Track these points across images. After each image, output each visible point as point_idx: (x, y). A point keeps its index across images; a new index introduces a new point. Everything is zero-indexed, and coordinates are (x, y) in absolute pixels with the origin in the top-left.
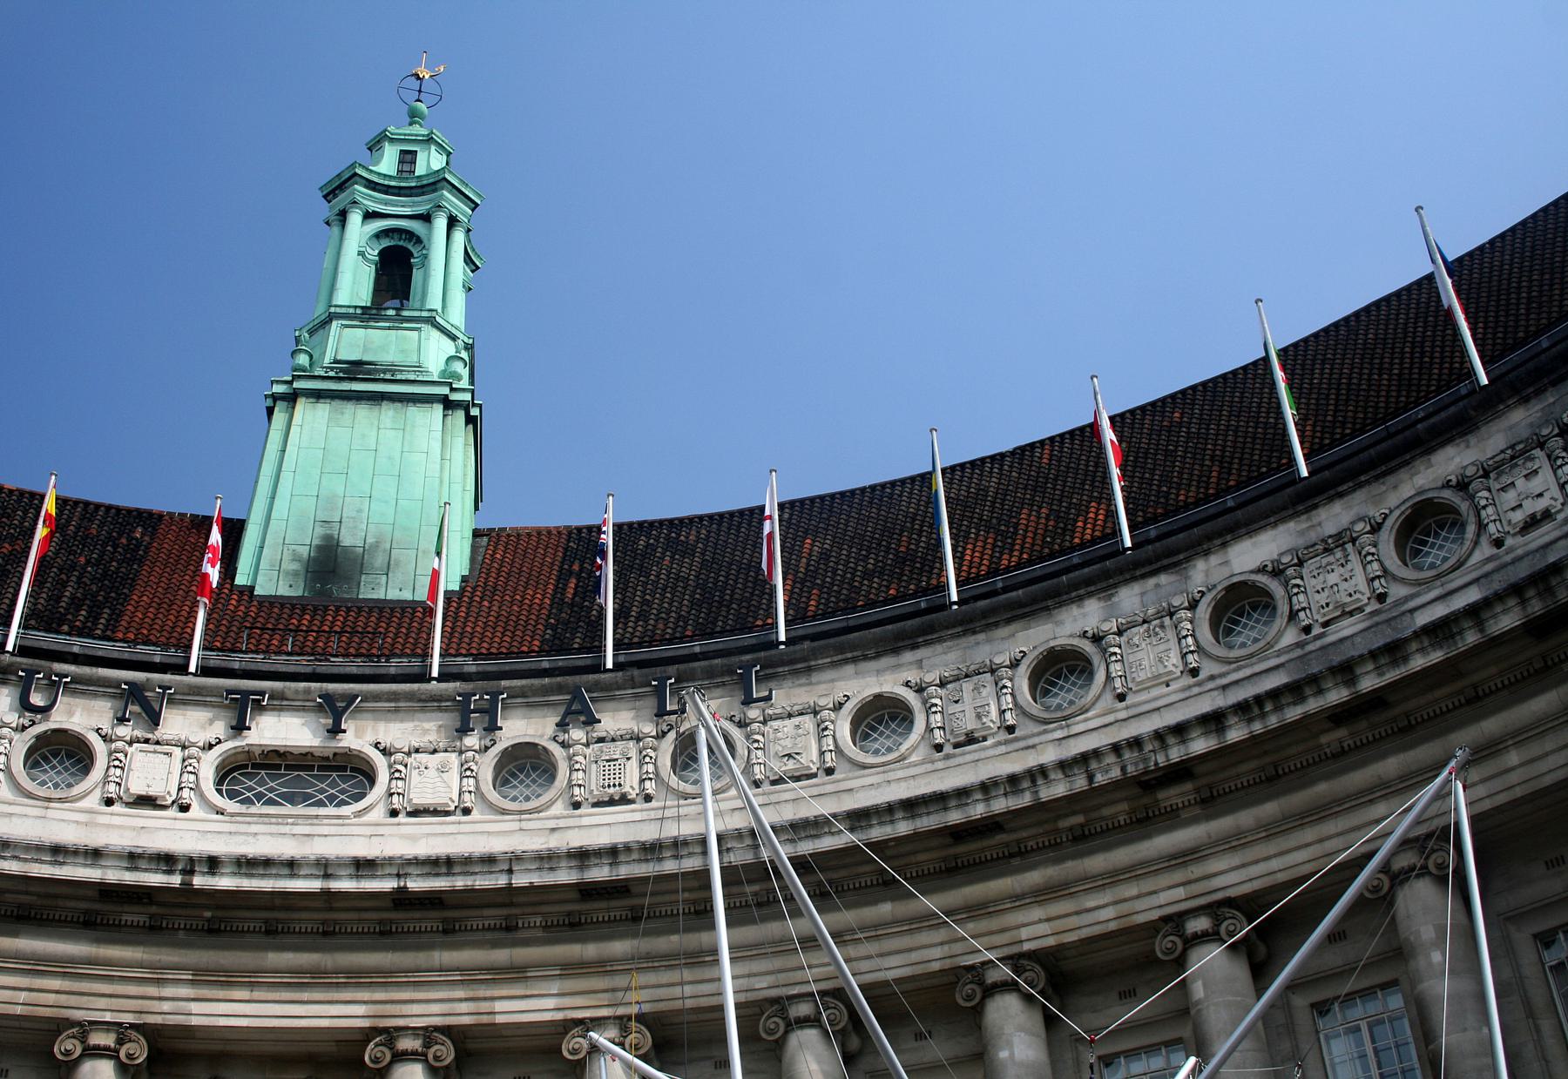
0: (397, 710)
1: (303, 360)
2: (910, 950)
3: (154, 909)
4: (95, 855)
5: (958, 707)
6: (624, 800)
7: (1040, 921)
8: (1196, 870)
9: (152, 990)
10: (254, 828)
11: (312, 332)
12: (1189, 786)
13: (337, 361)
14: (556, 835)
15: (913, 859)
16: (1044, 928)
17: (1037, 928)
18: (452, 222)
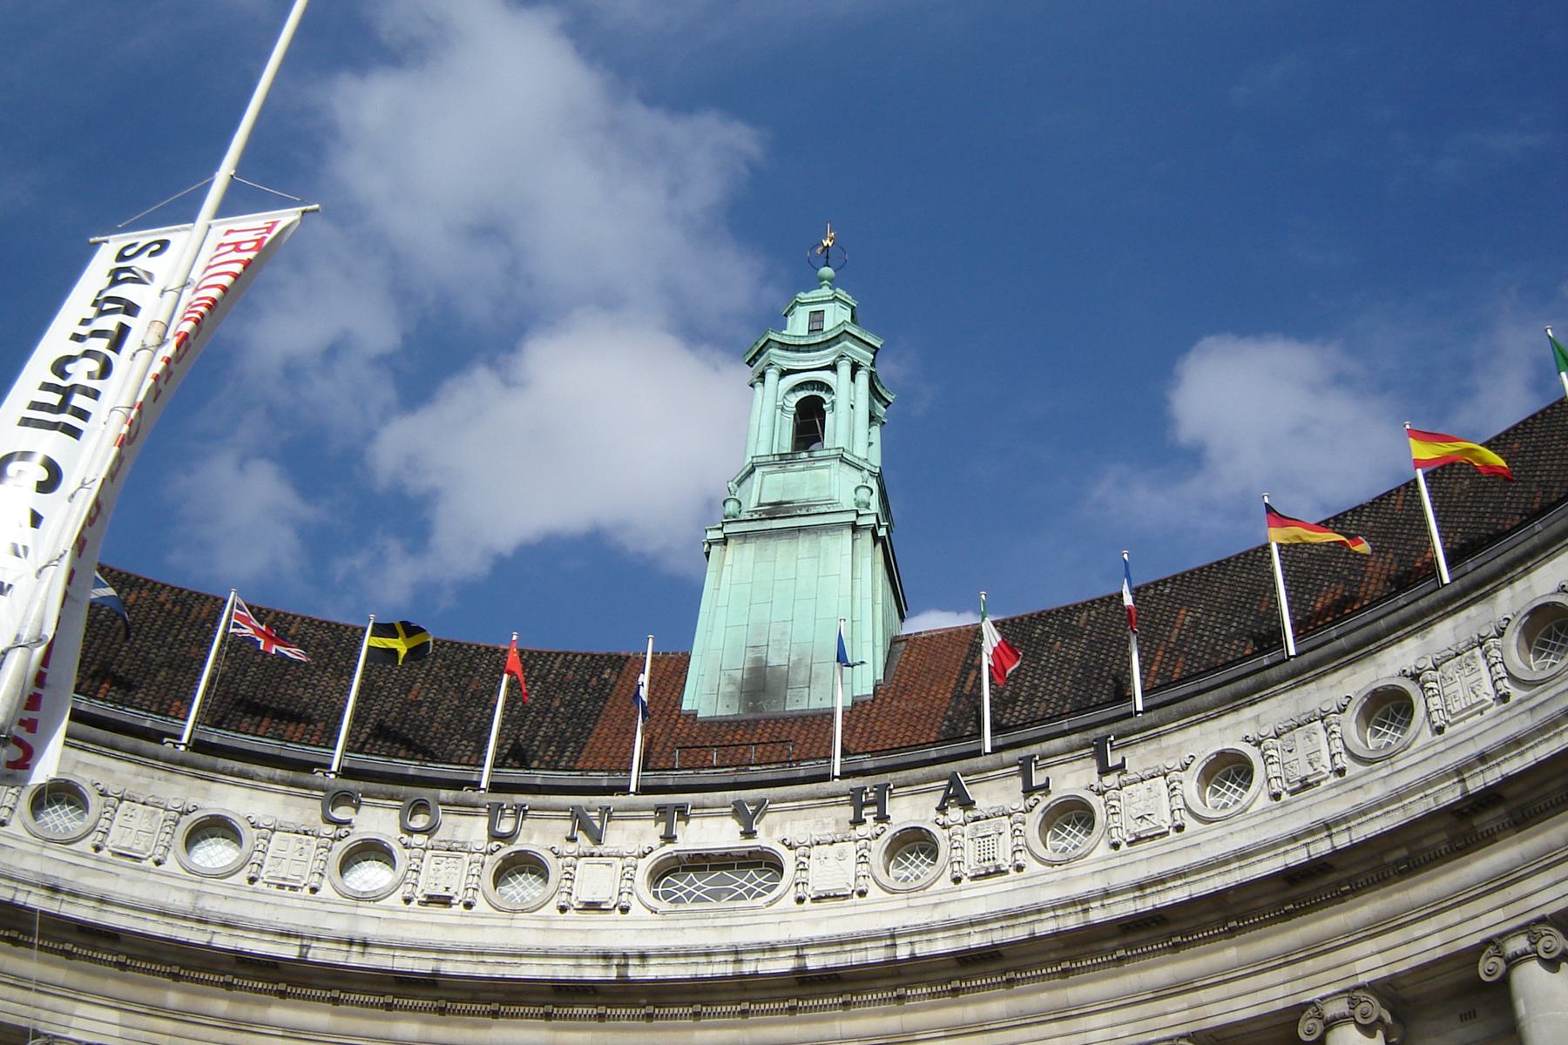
0: (801, 808)
1: (731, 507)
5: (1291, 756)
6: (999, 872)
7: (1373, 954)
10: (681, 924)
11: (739, 483)
12: (1501, 810)
13: (760, 505)
14: (940, 909)
16: (1377, 960)
17: (1372, 961)
18: (855, 367)
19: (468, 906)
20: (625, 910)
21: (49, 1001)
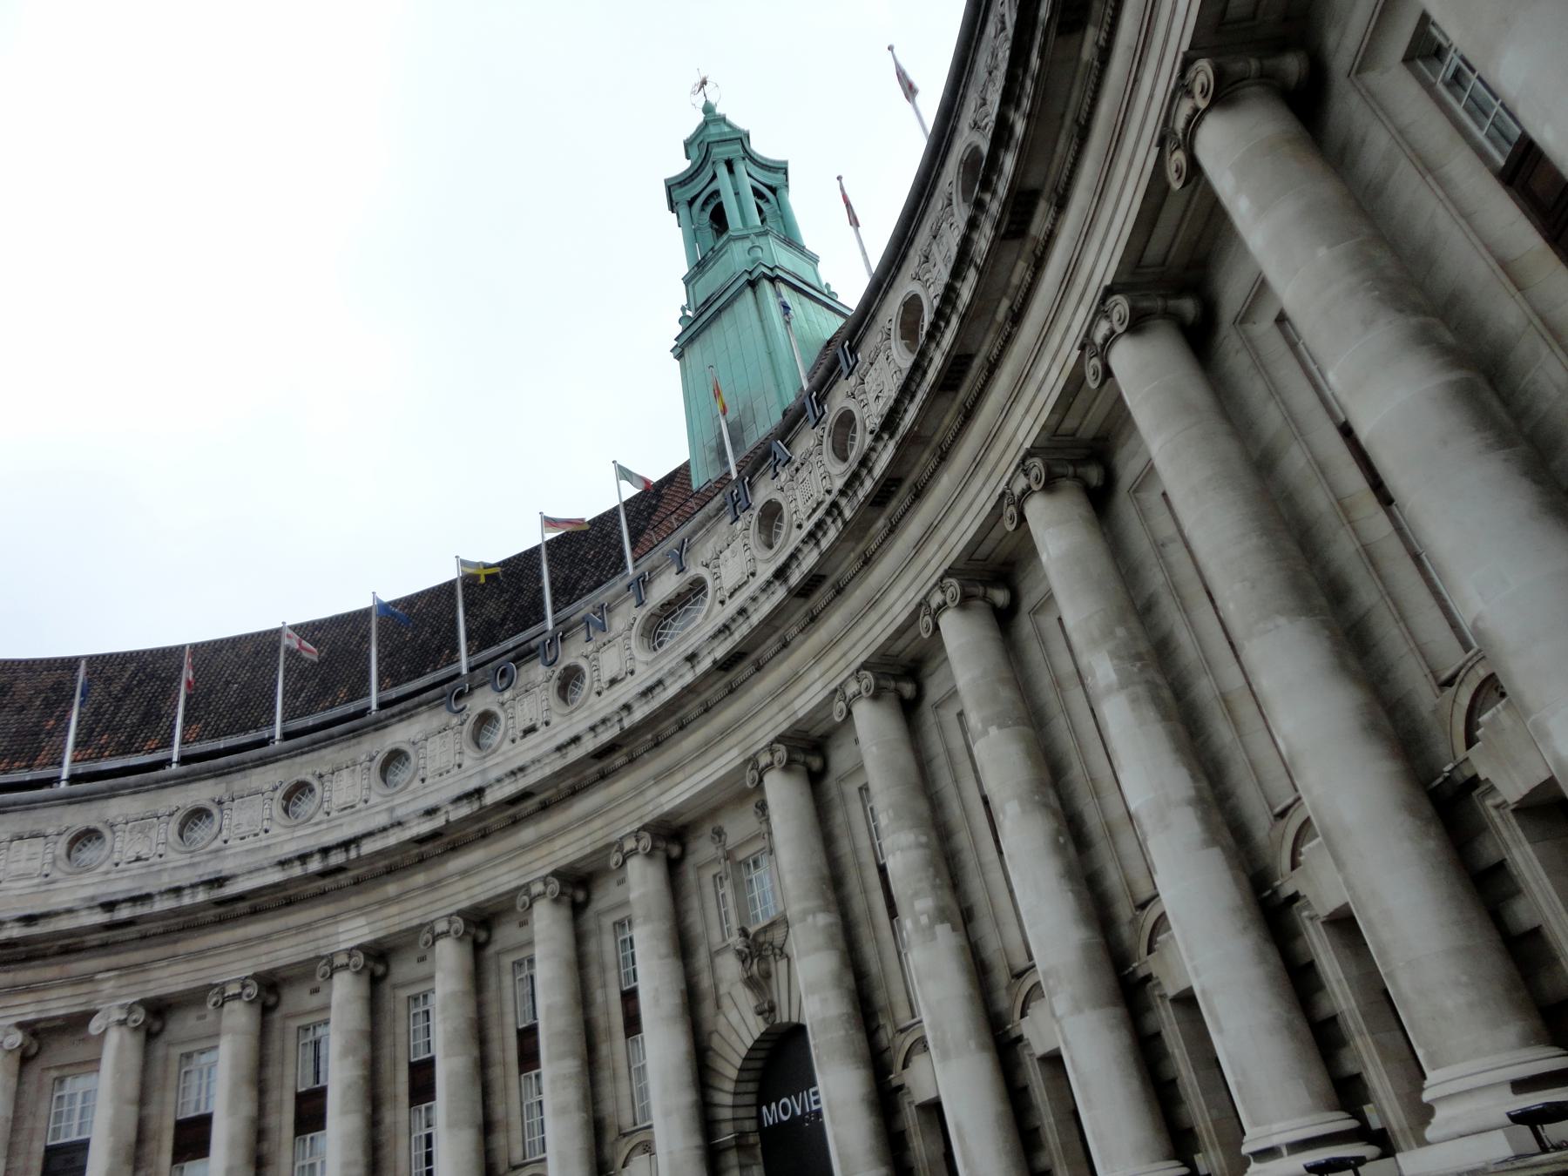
2: (971, 505)
3: (625, 750)
4: (576, 740)
8: (1081, 280)
9: (640, 800)
15: (943, 427)
19: (547, 724)
20: (632, 673)
21: (320, 933)
